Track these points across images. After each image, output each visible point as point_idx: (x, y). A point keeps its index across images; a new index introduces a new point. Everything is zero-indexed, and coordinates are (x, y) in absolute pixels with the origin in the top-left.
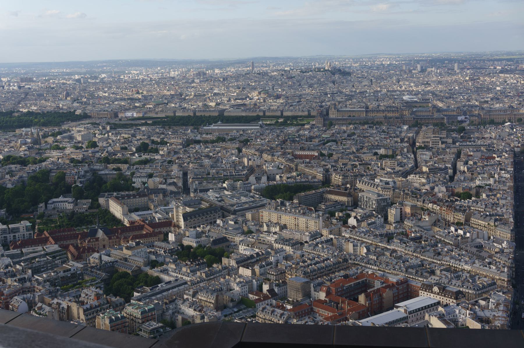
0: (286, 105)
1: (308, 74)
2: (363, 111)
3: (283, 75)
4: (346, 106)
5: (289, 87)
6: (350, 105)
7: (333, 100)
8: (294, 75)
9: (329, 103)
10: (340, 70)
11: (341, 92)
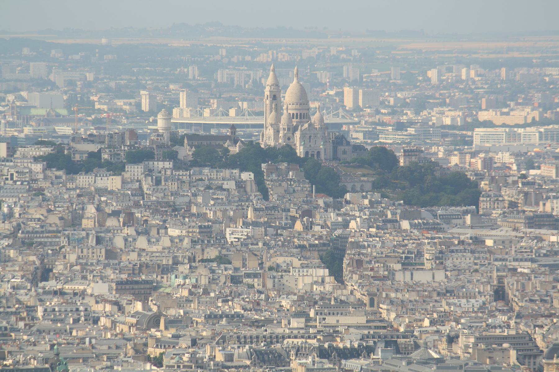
1: (113, 182)
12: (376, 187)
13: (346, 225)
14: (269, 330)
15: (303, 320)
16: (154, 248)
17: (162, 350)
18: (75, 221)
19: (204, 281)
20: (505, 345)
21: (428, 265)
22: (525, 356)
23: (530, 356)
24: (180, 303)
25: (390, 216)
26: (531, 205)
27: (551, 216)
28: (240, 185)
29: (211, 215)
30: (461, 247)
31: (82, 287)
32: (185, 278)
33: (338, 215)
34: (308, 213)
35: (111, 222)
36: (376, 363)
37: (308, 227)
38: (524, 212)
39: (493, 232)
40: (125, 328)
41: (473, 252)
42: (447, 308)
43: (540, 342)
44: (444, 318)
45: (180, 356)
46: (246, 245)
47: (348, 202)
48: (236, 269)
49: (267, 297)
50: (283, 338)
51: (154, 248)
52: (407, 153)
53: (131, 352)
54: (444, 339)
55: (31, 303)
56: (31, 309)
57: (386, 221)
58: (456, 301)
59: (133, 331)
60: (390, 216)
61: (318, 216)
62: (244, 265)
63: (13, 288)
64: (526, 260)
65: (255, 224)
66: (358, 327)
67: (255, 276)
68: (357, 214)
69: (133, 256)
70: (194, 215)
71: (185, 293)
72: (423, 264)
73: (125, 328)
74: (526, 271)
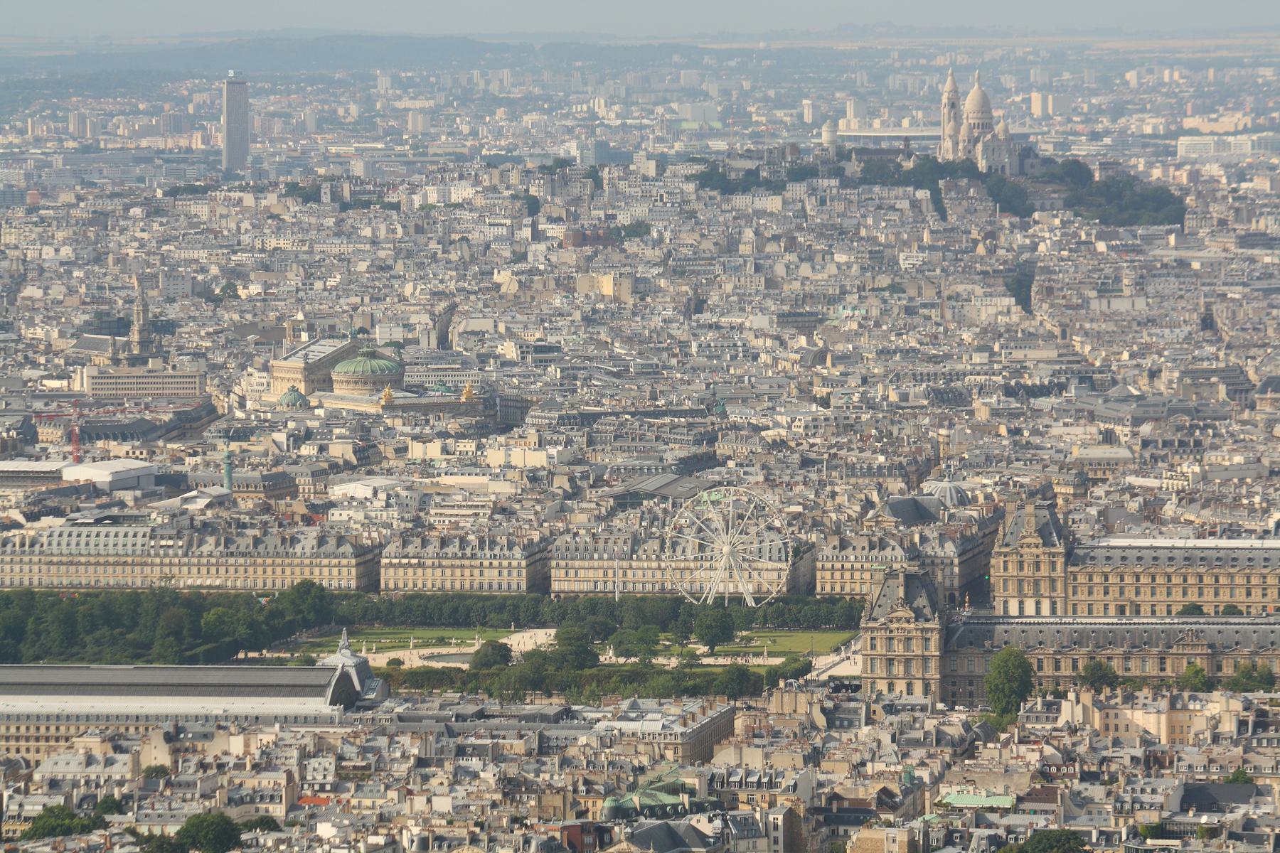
0: (575, 493)
1: (773, 203)
3: (533, 207)
6: (1186, 497)
8: (640, 211)
9: (981, 484)
10: (1075, 172)
12: (1068, 205)
13: (1034, 247)
14: (948, 367)
15: (987, 355)
16: (819, 277)
17: (829, 390)
18: (730, 247)
19: (875, 312)
20: (1214, 379)
21: (1127, 292)
22: (1236, 391)
23: (1241, 391)
24: (848, 337)
25: (1084, 237)
26: (1242, 222)
27: (1265, 234)
28: (915, 204)
29: (882, 239)
30: (1165, 271)
31: (739, 321)
32: (854, 309)
33: (1025, 237)
34: (992, 235)
35: (771, 248)
36: (1069, 401)
37: (992, 251)
38: (1235, 230)
39: (1200, 254)
40: (788, 366)
41: (1177, 276)
42: (1148, 339)
43: (1252, 375)
44: (1145, 350)
45: (849, 395)
46: (922, 271)
47: (1036, 222)
48: (911, 299)
49: (946, 330)
50: (965, 375)
51: (819, 277)
52: (1103, 166)
53: (795, 392)
54: (1145, 374)
55: (684, 338)
56: (684, 345)
57: (1080, 243)
58: (1158, 331)
59: (797, 368)
60: (1084, 237)
61: (1002, 239)
62: (920, 294)
63: (665, 321)
64: (1237, 284)
65: (932, 248)
66: (1049, 362)
67: (933, 306)
68: (1047, 235)
69: (796, 285)
70: (863, 238)
71: (854, 326)
72: (1121, 291)
73: (788, 366)
74: (1237, 296)
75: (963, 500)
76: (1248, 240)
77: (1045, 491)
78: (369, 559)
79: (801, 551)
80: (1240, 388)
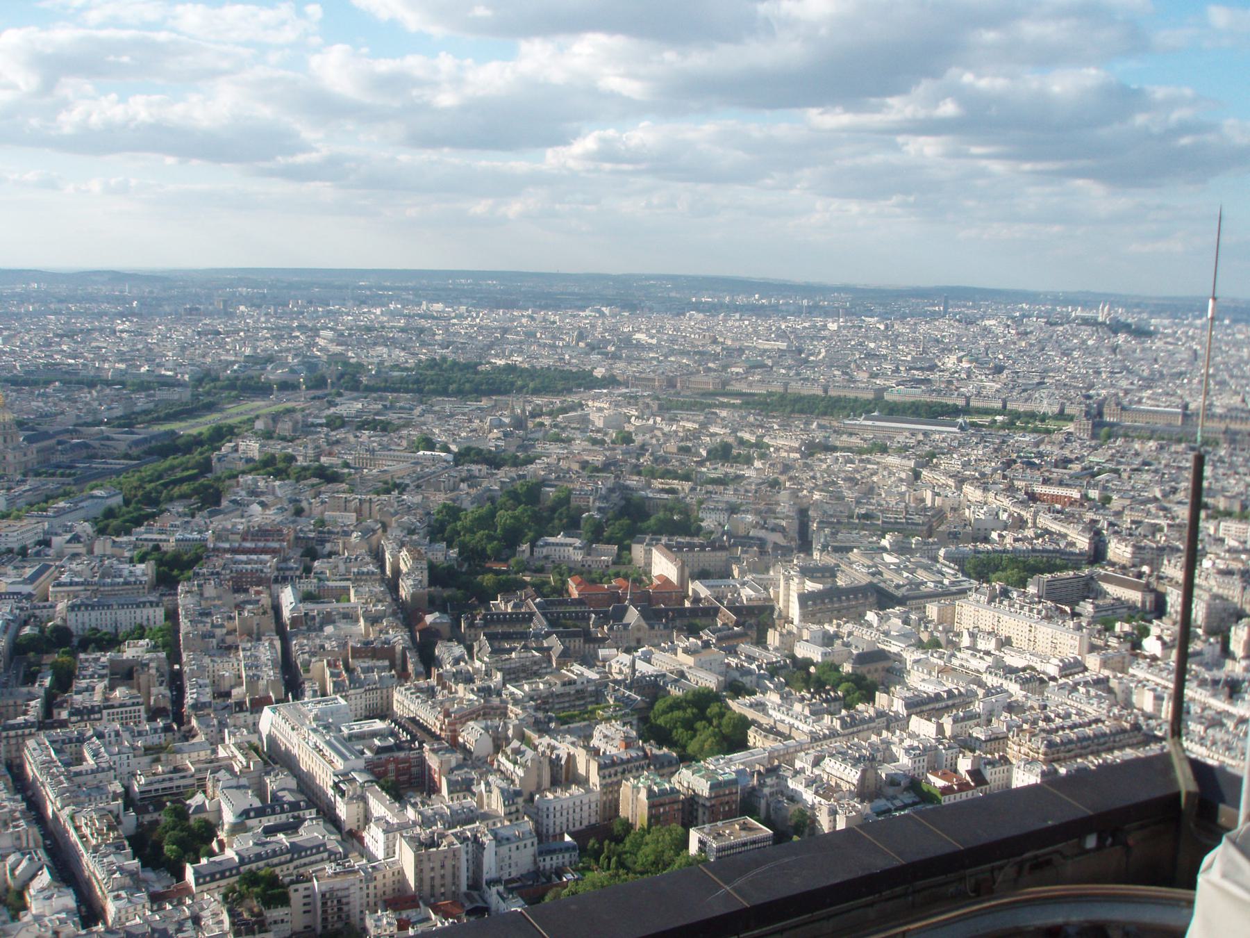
1: (1061, 328)
2: (1176, 413)
4: (1140, 402)
5: (1020, 351)
6: (1149, 398)
7: (1112, 385)
9: (1103, 392)
11: (1130, 372)
75: (1098, 395)
76: (1166, 343)
77: (1116, 395)
78: (968, 399)
79: (1063, 405)
80: (1162, 375)
